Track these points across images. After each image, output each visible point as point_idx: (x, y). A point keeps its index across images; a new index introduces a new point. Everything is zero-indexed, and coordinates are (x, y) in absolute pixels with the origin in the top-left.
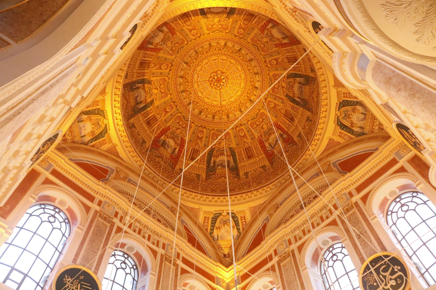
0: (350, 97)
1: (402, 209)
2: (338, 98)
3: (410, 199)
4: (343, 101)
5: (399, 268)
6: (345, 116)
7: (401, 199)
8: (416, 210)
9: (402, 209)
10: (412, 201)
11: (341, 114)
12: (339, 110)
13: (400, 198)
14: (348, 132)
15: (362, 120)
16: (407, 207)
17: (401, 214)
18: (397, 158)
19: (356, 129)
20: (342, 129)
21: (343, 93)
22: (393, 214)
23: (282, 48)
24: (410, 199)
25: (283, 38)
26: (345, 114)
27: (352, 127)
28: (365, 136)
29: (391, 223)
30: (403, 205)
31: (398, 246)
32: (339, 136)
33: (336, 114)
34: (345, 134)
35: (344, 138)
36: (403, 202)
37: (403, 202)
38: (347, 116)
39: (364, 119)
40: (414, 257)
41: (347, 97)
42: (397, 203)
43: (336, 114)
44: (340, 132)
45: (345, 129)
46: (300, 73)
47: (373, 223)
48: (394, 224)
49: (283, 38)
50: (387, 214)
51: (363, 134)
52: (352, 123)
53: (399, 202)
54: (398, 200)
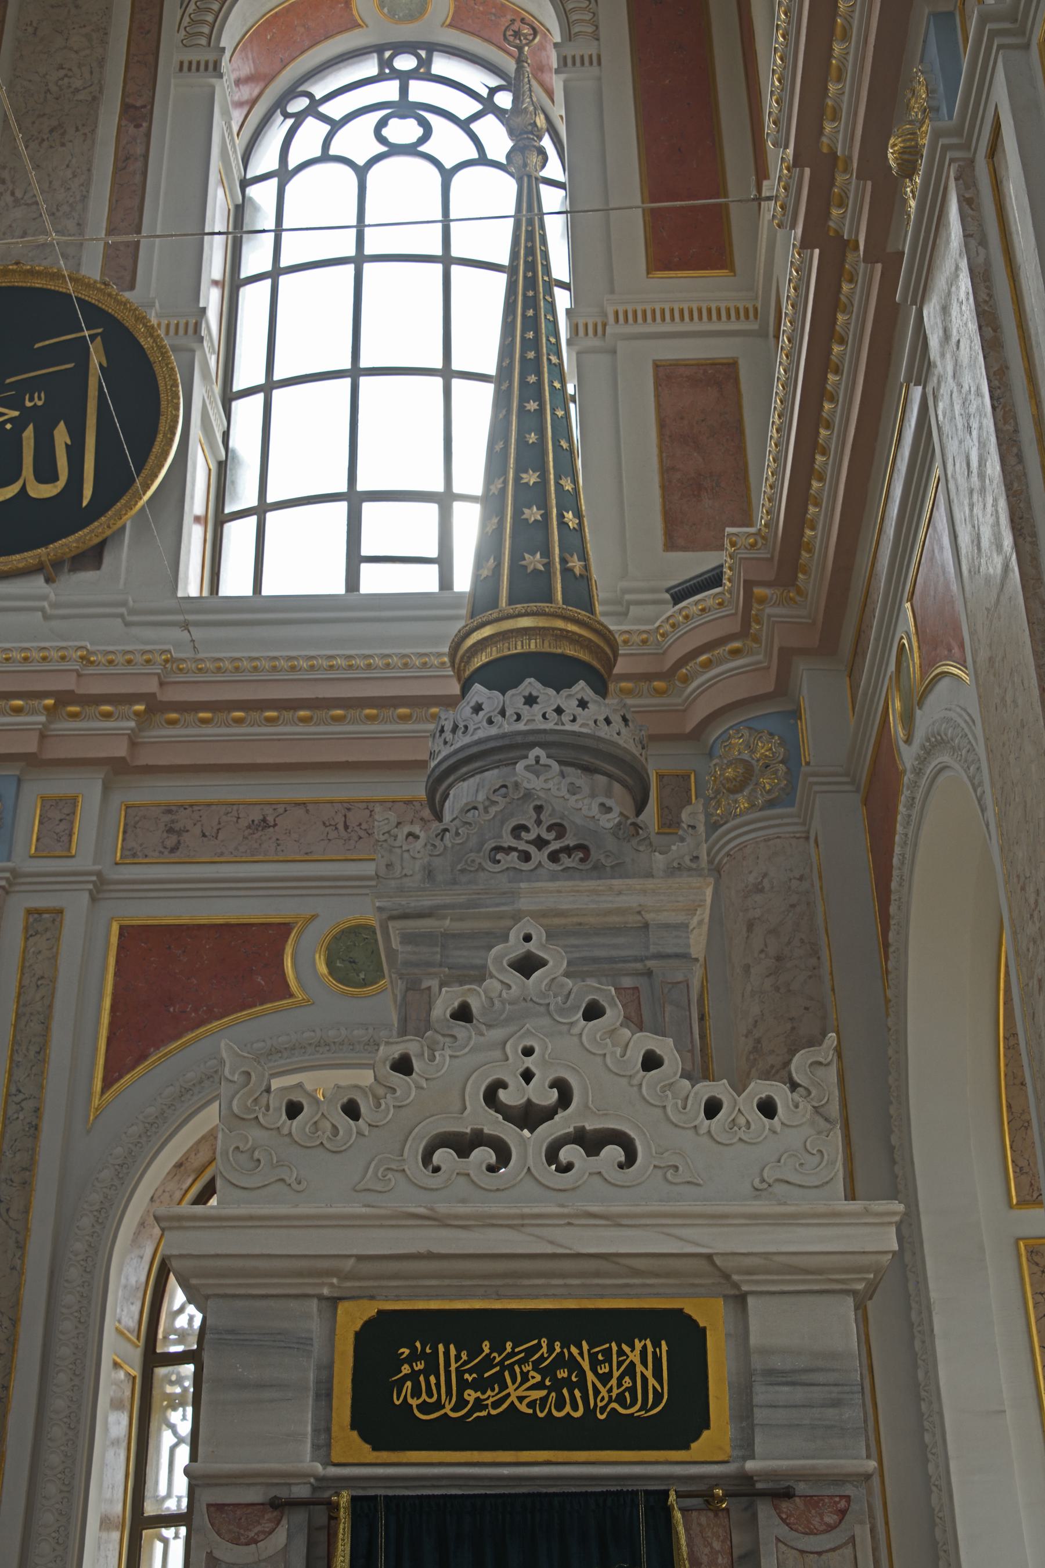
1: (382, 123)
9: (382, 123)
10: (465, 125)
13: (425, 63)
16: (419, 132)
22: (310, 122)
29: (266, 159)
30: (404, 108)
31: (212, 300)
36: (420, 91)
37: (420, 91)
40: (247, 413)
47: (172, 90)
48: (284, 174)
50: (280, 105)
53: (404, 78)
54: (405, 63)
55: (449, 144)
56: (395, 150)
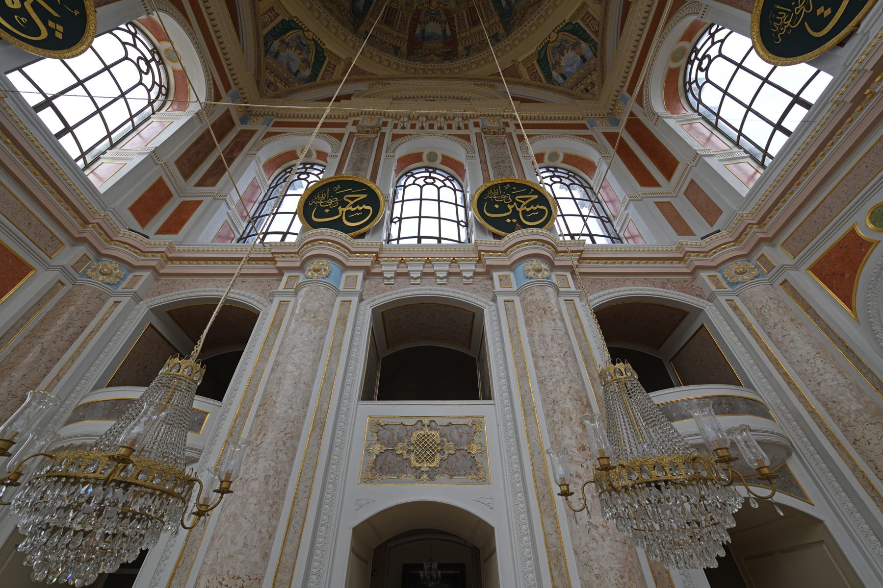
0: (326, 70)
2: (331, 52)
3: (157, 80)
4: (325, 57)
5: (59, 35)
6: (301, 42)
7: (158, 64)
8: (141, 87)
11: (306, 38)
12: (313, 39)
14: (274, 28)
15: (288, 64)
17: (133, 54)
18: (230, 92)
19: (276, 44)
20: (282, 21)
21: (335, 66)
23: (412, 17)
24: (157, 80)
25: (423, 31)
26: (304, 45)
27: (283, 42)
28: (263, 53)
32: (272, 9)
33: (308, 30)
34: (272, 21)
35: (266, 13)
38: (301, 46)
39: (289, 69)
41: (328, 66)
42: (150, 51)
43: (308, 30)
44: (278, 15)
45: (281, 26)
46: (370, 12)
49: (423, 31)
51: (267, 51)
52: (288, 45)
55: (147, 80)
56: (138, 66)
